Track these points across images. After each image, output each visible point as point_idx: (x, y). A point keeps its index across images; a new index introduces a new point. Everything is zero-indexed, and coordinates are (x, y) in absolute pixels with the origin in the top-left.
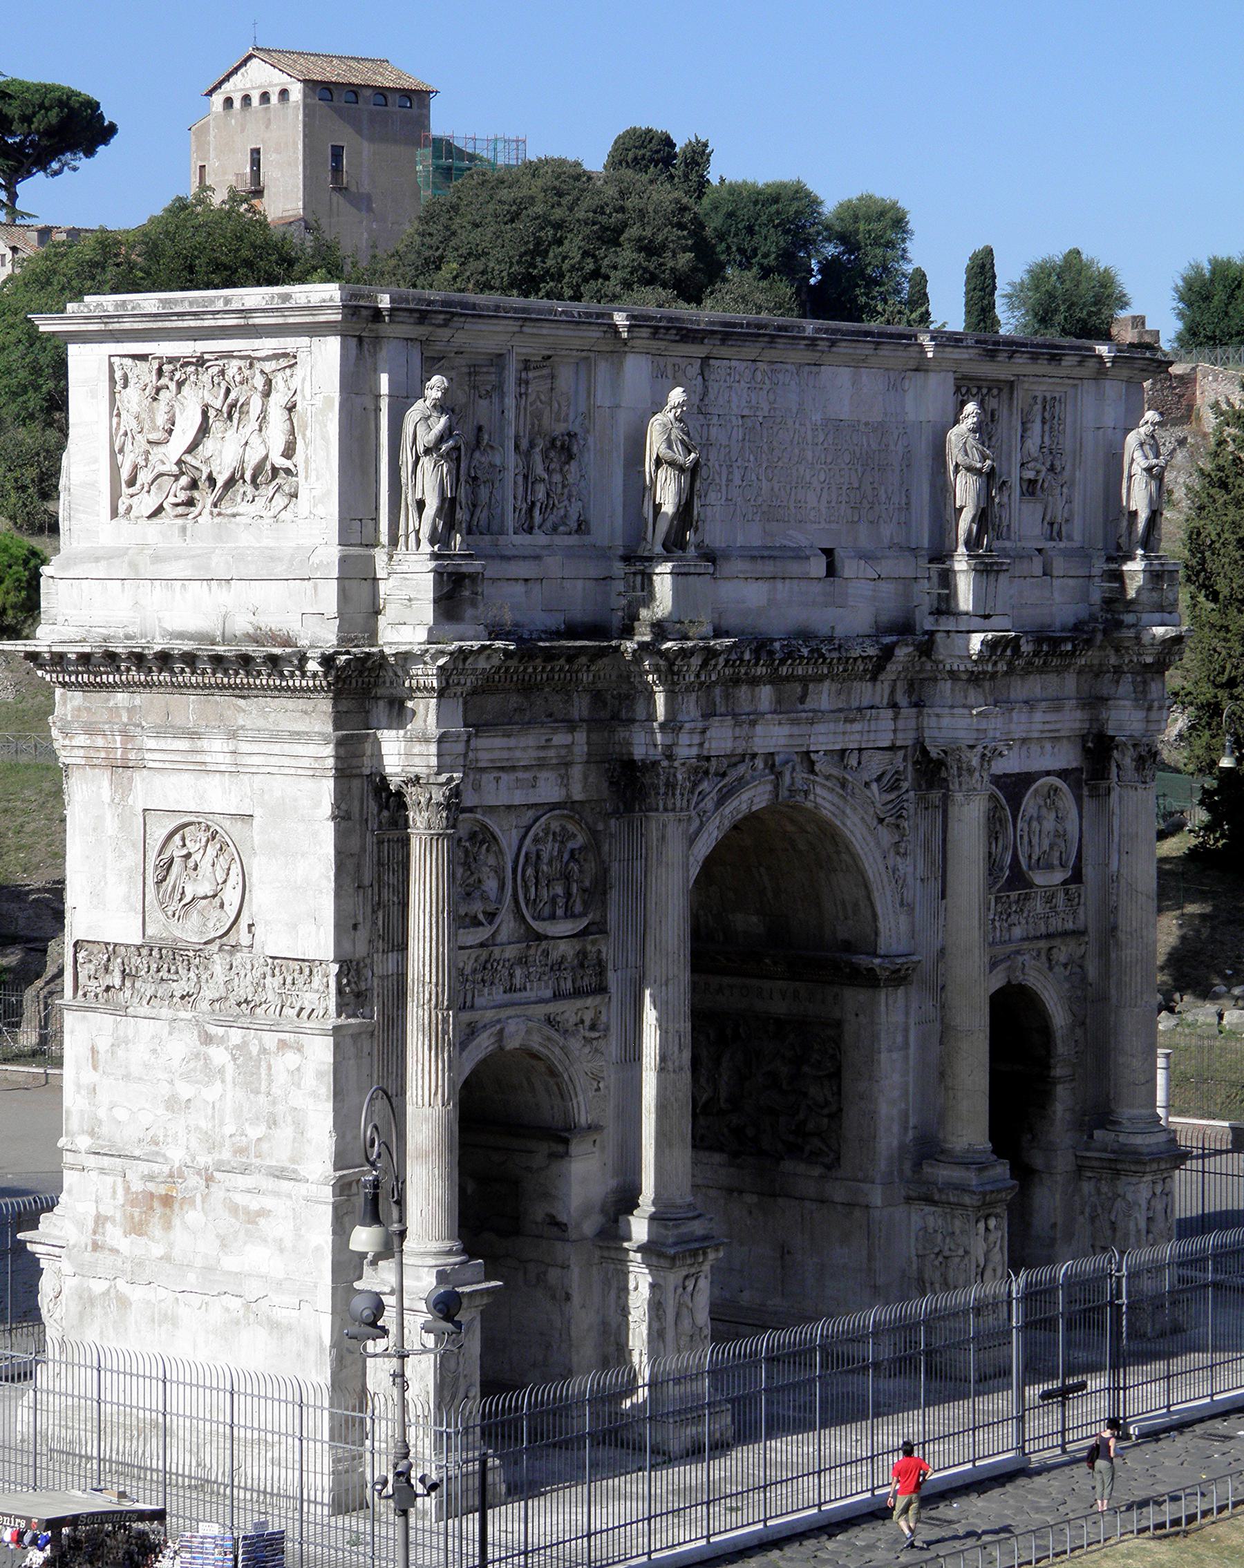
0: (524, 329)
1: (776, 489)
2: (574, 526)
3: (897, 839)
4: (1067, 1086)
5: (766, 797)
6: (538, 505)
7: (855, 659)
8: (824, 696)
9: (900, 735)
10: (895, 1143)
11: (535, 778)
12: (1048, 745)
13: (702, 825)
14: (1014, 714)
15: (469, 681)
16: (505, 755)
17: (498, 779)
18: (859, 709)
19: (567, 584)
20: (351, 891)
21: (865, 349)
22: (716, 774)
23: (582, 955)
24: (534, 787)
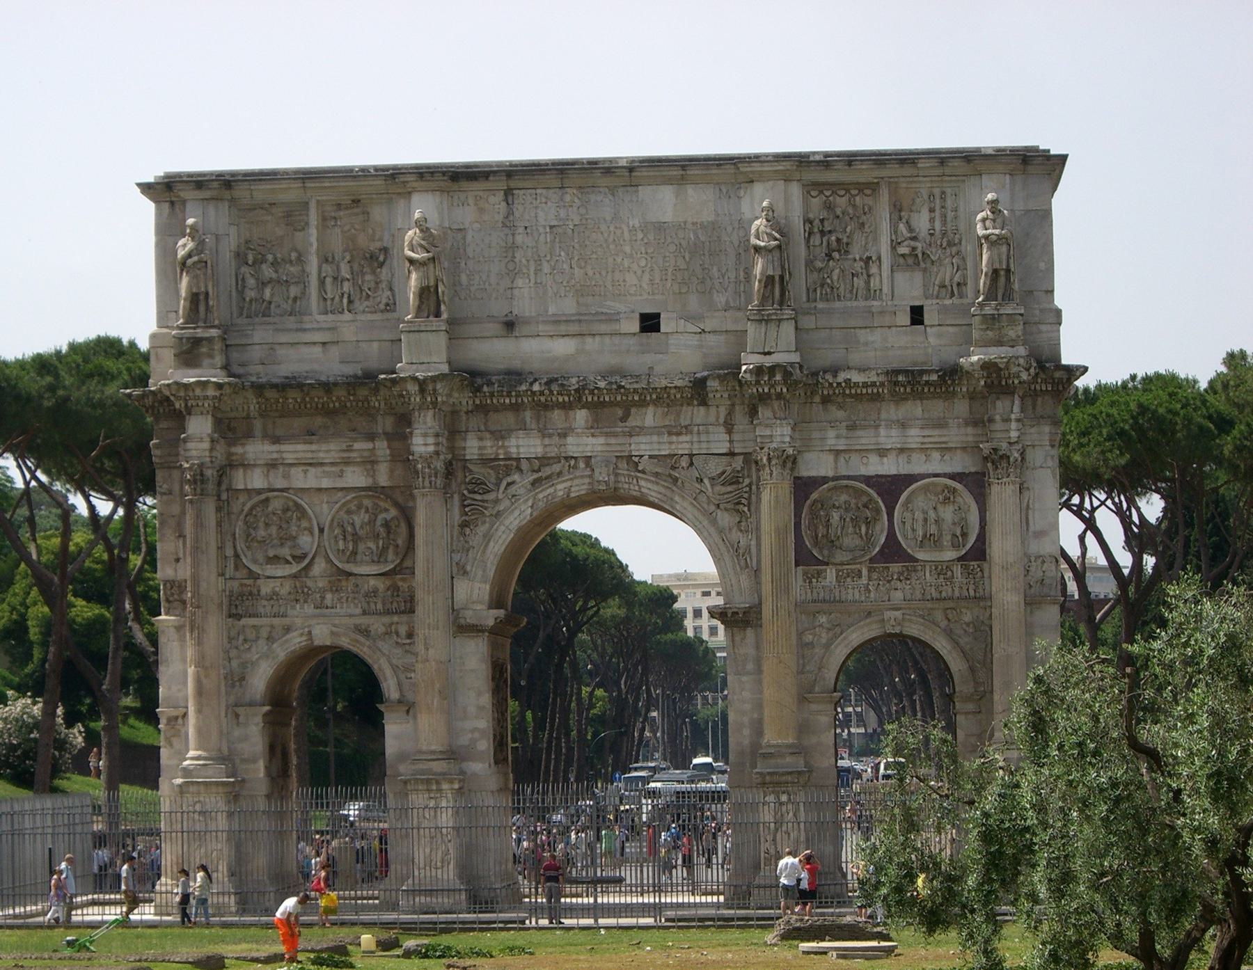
0: (306, 185)
1: (590, 273)
2: (382, 306)
3: (738, 519)
4: (970, 716)
5: (585, 487)
6: (346, 296)
7: (666, 387)
8: (650, 417)
9: (736, 445)
10: (746, 742)
11: (342, 471)
12: (936, 455)
13: (513, 504)
14: (882, 431)
15: (206, 405)
16: (310, 455)
17: (305, 472)
18: (686, 427)
19: (360, 344)
20: (172, 538)
21: (677, 172)
22: (534, 471)
23: (395, 588)
24: (341, 476)
